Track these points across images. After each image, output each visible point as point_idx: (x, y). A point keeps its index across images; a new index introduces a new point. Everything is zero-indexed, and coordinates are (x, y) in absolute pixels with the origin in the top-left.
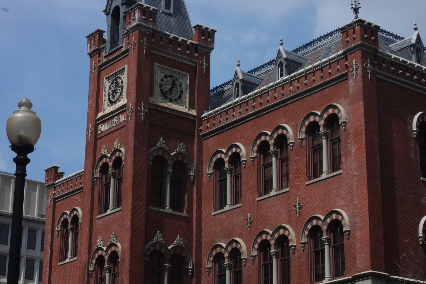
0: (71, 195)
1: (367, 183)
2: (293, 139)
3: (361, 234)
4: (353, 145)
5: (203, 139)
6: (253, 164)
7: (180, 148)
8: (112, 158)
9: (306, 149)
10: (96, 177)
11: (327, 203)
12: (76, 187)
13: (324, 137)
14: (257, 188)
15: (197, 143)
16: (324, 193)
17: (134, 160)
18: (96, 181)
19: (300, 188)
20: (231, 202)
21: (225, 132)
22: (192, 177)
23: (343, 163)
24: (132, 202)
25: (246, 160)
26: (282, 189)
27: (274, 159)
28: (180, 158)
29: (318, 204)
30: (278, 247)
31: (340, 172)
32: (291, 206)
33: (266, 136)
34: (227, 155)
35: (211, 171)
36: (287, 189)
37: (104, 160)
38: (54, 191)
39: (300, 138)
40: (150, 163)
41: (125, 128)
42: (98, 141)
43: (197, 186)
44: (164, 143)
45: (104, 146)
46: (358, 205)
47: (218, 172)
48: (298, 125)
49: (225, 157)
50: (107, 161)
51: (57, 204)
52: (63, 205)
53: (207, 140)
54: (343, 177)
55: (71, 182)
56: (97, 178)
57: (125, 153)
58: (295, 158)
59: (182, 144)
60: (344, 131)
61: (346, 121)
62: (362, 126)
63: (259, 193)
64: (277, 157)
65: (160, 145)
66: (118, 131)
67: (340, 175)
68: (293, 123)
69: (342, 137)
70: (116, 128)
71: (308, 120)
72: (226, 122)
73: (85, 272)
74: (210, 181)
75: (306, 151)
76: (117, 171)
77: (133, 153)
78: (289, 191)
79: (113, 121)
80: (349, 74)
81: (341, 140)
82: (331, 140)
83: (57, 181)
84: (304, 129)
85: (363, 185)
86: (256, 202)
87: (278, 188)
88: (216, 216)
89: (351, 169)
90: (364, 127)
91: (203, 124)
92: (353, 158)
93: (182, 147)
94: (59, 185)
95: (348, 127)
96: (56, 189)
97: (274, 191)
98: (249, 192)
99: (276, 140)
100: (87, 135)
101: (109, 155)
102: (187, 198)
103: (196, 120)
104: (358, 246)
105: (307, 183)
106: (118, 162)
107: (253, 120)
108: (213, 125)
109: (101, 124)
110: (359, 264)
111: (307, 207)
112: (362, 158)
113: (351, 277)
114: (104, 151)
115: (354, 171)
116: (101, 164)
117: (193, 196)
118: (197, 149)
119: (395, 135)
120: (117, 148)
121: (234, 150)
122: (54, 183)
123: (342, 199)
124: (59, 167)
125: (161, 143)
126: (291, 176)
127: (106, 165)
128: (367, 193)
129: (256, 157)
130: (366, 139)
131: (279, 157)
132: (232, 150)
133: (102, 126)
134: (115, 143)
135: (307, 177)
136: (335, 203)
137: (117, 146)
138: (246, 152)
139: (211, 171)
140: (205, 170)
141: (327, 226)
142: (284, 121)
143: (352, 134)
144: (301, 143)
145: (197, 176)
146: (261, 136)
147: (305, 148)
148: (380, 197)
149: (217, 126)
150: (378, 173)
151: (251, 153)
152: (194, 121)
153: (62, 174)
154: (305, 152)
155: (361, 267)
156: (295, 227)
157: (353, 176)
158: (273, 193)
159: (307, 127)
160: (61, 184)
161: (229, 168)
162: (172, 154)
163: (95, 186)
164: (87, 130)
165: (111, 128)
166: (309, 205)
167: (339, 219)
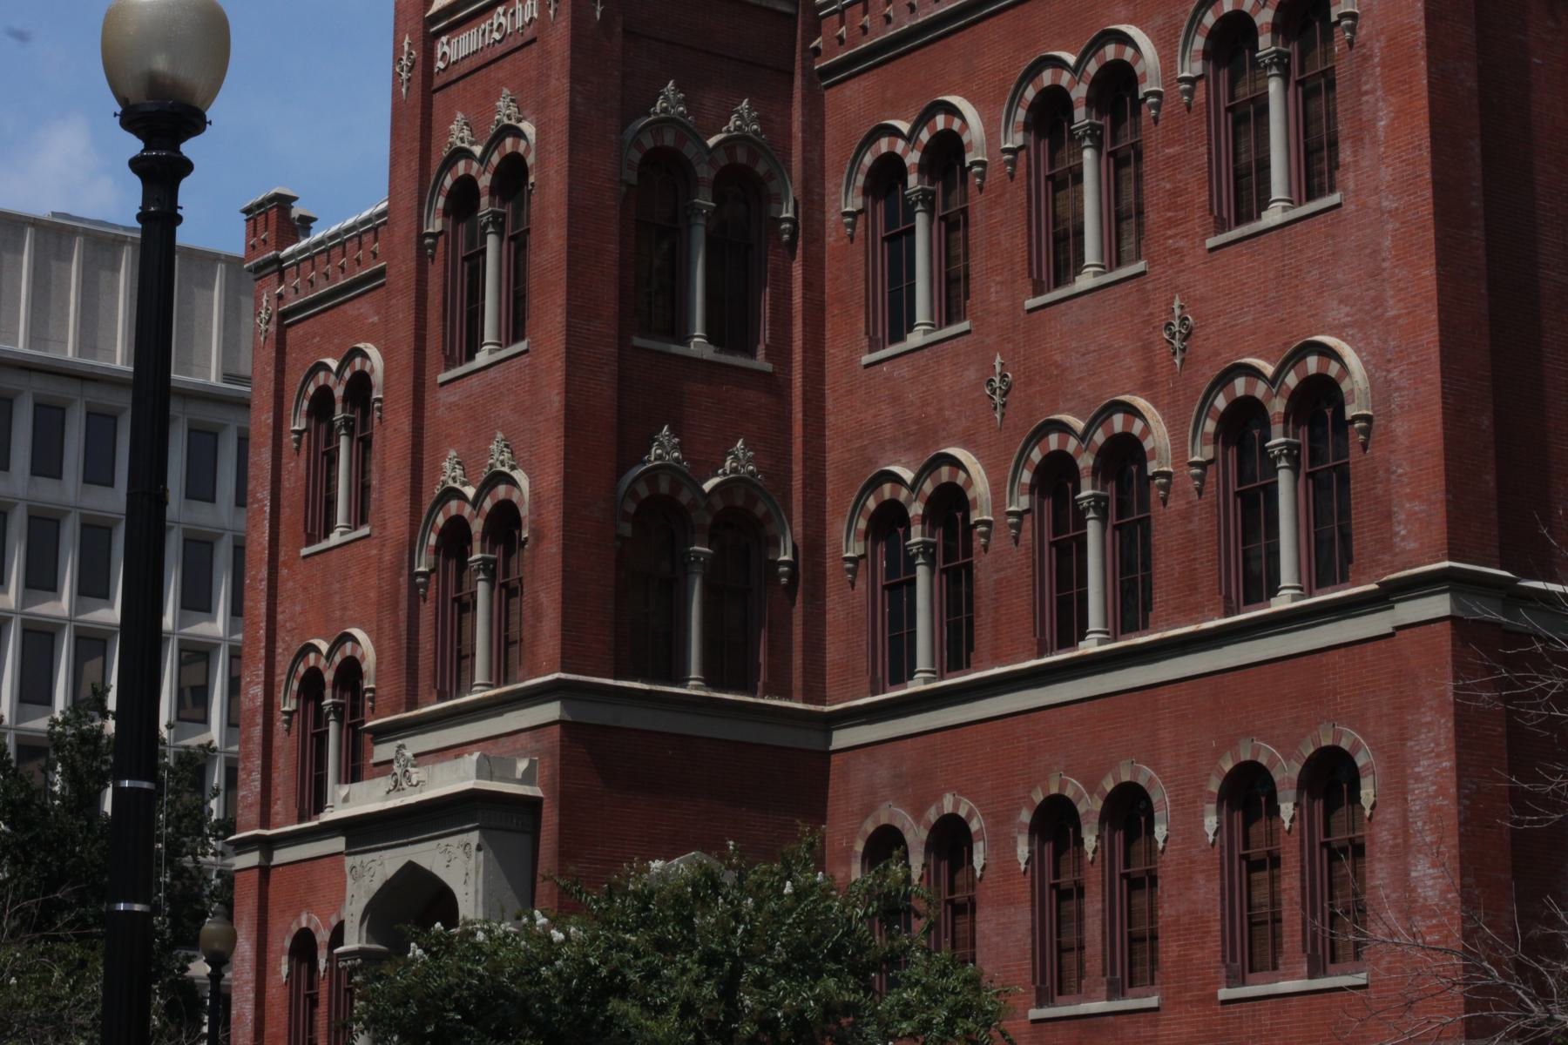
0: (341, 299)
1: (1433, 241)
2: (1158, 79)
3: (1414, 427)
4: (1383, 100)
5: (823, 84)
6: (1012, 176)
7: (741, 117)
8: (489, 160)
9: (1209, 118)
10: (430, 230)
11: (1284, 316)
12: (357, 268)
13: (1274, 71)
14: (1026, 262)
15: (804, 98)
16: (1275, 278)
17: (570, 167)
18: (433, 246)
19: (1188, 260)
20: (932, 317)
21: (907, 58)
22: (788, 225)
23: (1344, 165)
24: (567, 321)
25: (986, 159)
26: (1119, 264)
27: (1088, 154)
28: (741, 157)
29: (1254, 319)
30: (1105, 481)
31: (1335, 198)
32: (1154, 328)
33: (1058, 70)
34: (915, 142)
35: (854, 203)
36: (1140, 266)
37: (461, 167)
38: (279, 285)
39: (1186, 74)
40: (632, 177)
41: (534, 46)
42: (437, 96)
43: (805, 259)
44: (679, 102)
45: (460, 116)
46: (1400, 321)
47: (881, 206)
48: (1177, 28)
49: (905, 151)
50: (473, 173)
51: (291, 334)
52: (314, 337)
53: (839, 87)
54: (1345, 220)
55: (339, 250)
56: (434, 236)
57: (537, 139)
58: (1167, 151)
59: (748, 103)
60: (1348, 49)
61: (1357, 11)
62: (1414, 28)
63: (1033, 280)
64: (1098, 147)
65: (664, 110)
66: (509, 59)
67: (1334, 211)
68: (1159, 20)
69: (1343, 72)
70: (500, 49)
71: (1213, 7)
72: (909, 20)
73: (401, 579)
74: (852, 240)
75: (1209, 125)
76: (508, 209)
77: (565, 138)
78: (1143, 273)
79: (490, 21)
81: (1337, 82)
82: (1299, 83)
83: (289, 250)
84: (1199, 43)
85: (1421, 248)
86: (1022, 314)
87: (1106, 263)
88: (878, 367)
89: (1376, 190)
90: (1422, 33)
91: (824, 29)
92: (1382, 149)
93: (746, 115)
94: (297, 264)
95: (1362, 33)
96: (287, 278)
97: (1091, 274)
98: (998, 279)
99: (1096, 83)
100: (396, 76)
101: (478, 150)
102: (767, 302)
103: (797, 13)
104: (1400, 471)
105: (1211, 242)
106: (512, 175)
107: (1011, 11)
108: (861, 31)
109: (445, 35)
110: (1404, 538)
111: (1213, 332)
112: (1414, 148)
113: (1373, 586)
114: (458, 133)
115: (1387, 198)
116: (448, 182)
117: (790, 294)
118: (804, 123)
119: (1539, 62)
120: (506, 121)
121: (940, 121)
122: (277, 256)
123: (1341, 302)
124: (295, 199)
125: (669, 100)
126: (1152, 216)
127: (466, 186)
128: (1435, 276)
129: (1021, 148)
130: (1429, 77)
131: (1107, 148)
132: (931, 123)
133: (448, 43)
134: (500, 104)
135: (1211, 220)
136: (1317, 315)
137: (509, 117)
138: (985, 132)
139: (854, 203)
140: (833, 197)
141: (1285, 401)
142: (1123, 12)
143: (1377, 60)
144: (1190, 93)
145: (804, 220)
146: (1040, 72)
147: (1205, 114)
148: (1483, 291)
149: (877, 35)
150: (1474, 204)
151: (1002, 135)
152: (792, 18)
153: (306, 222)
154: (1205, 127)
155: (1410, 551)
156: (1168, 404)
157: (1382, 215)
158: (1085, 281)
159: (1212, 35)
160: (303, 260)
161: (922, 190)
162: (712, 142)
163: (430, 264)
164: (394, 58)
165: (485, 49)
166: (1221, 323)
167: (1329, 374)
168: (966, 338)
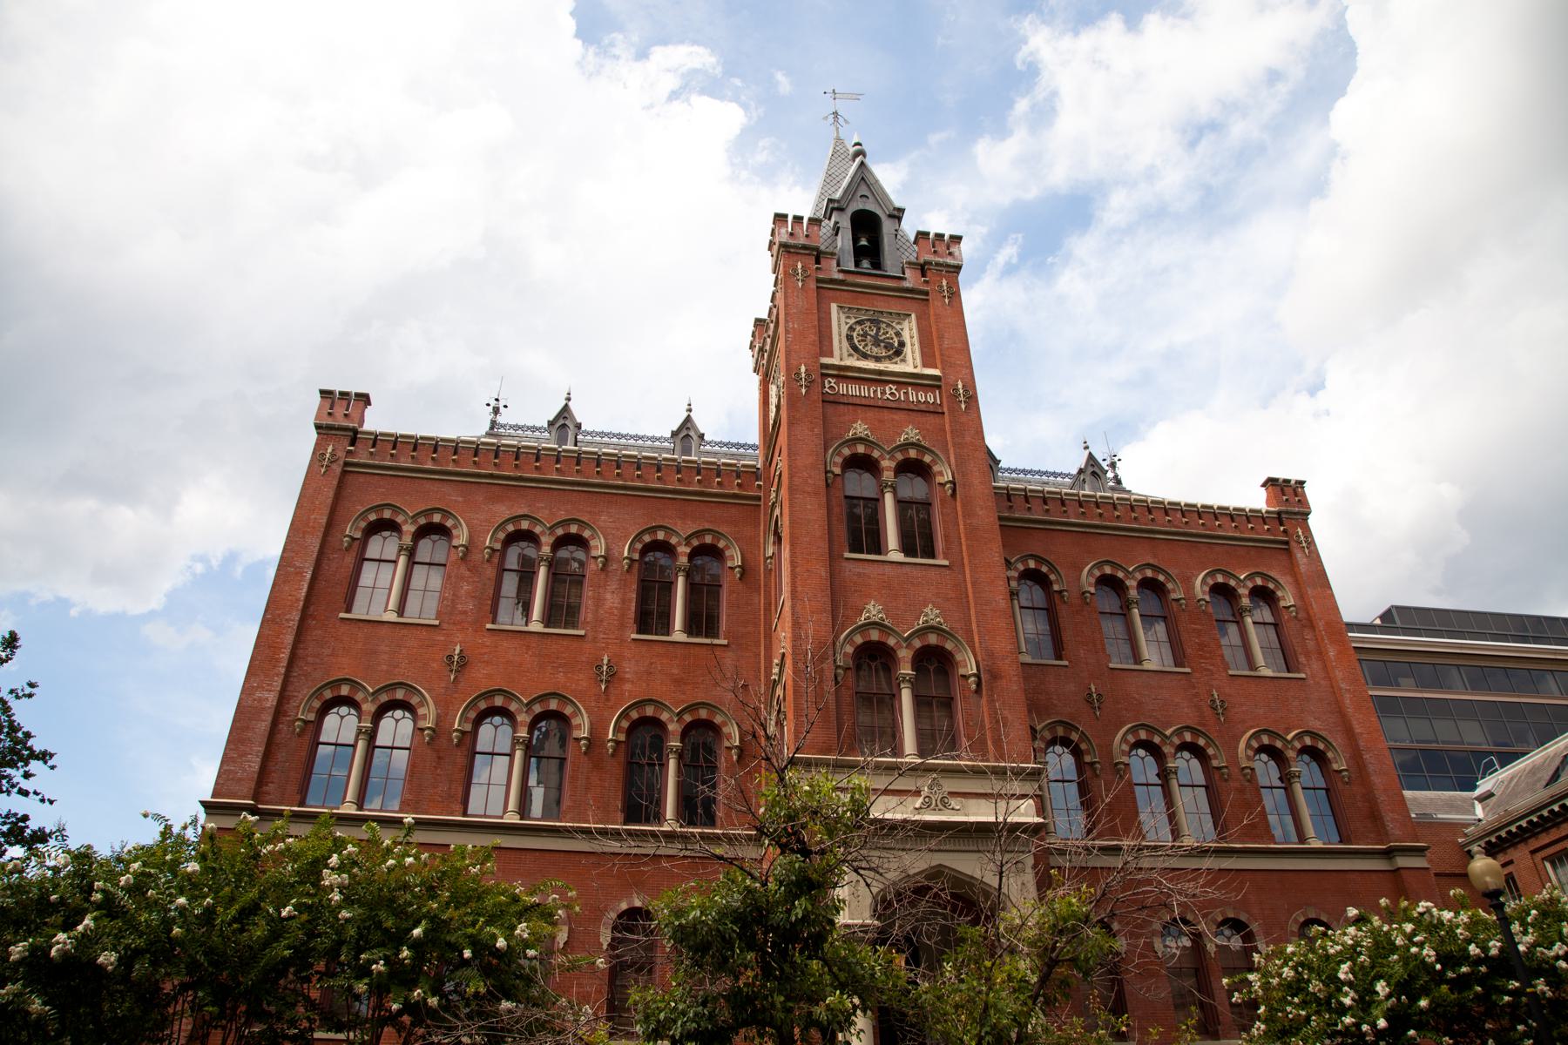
31: (1303, 676)
36: (1187, 670)
73: (825, 666)
80: (1293, 544)
105: (1231, 672)
168: (1065, 669)
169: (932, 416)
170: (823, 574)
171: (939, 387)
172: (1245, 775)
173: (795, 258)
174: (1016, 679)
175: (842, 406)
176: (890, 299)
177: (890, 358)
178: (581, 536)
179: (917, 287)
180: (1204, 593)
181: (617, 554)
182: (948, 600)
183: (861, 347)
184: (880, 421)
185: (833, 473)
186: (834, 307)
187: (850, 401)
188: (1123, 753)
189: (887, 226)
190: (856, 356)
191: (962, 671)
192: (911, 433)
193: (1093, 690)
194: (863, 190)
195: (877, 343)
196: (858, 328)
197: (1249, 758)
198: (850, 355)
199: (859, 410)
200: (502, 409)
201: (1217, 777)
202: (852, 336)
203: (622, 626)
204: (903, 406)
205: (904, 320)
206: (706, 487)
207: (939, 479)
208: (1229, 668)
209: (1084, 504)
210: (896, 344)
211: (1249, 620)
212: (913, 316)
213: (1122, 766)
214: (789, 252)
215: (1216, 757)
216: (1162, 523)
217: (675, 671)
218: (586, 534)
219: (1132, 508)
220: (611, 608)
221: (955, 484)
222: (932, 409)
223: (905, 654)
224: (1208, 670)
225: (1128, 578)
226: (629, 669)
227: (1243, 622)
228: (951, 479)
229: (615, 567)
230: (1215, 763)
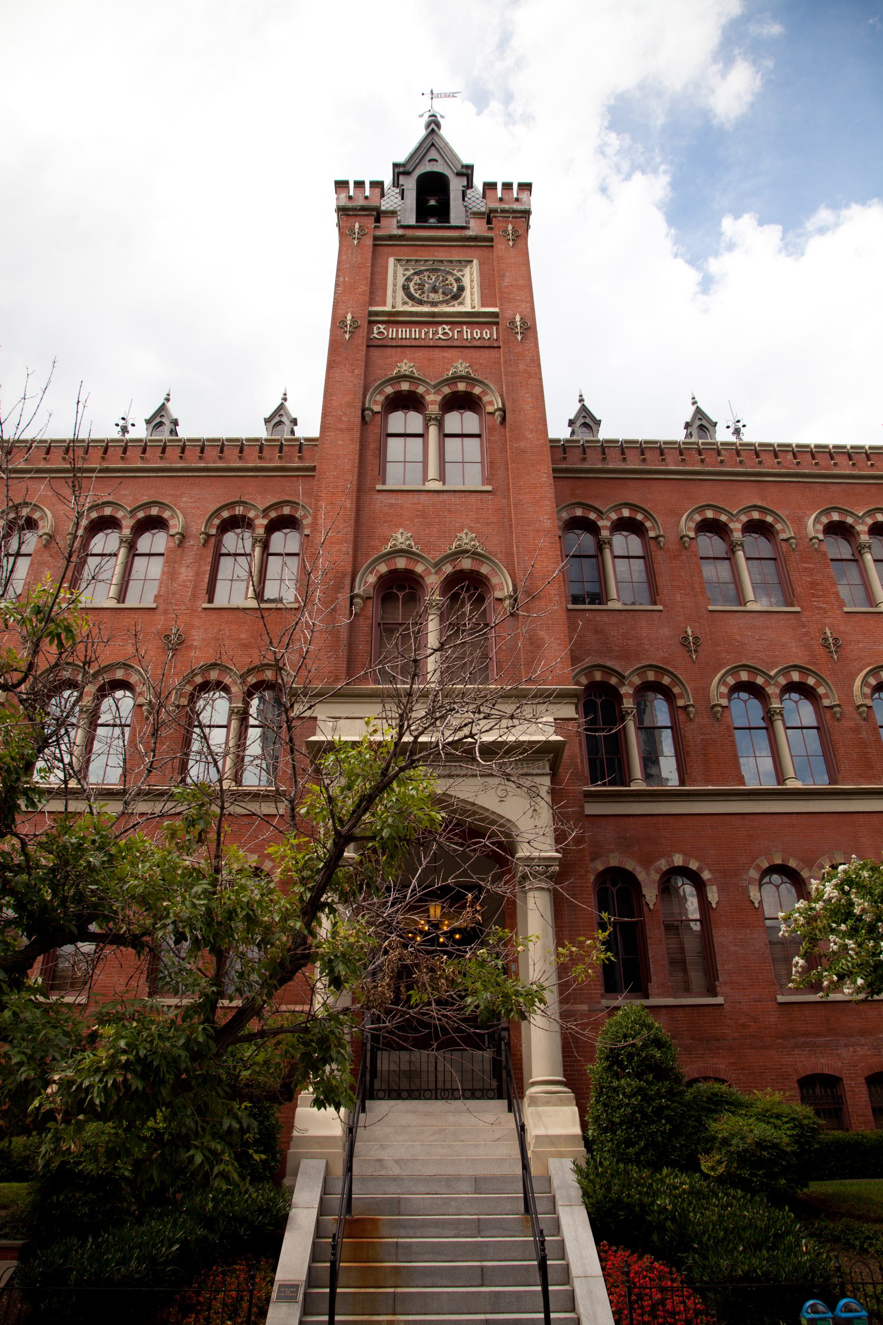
88: (580, 613)
105: (846, 609)
168: (658, 614)
169: (486, 351)
170: (348, 506)
171: (497, 324)
172: (860, 714)
173: (353, 219)
174: (557, 598)
175: (390, 349)
176: (452, 249)
177: (446, 302)
178: (161, 517)
179: (480, 234)
180: (817, 531)
181: (194, 532)
182: (488, 524)
183: (417, 295)
184: (429, 360)
185: (372, 410)
186: (391, 261)
187: (400, 343)
188: (722, 695)
189: (456, 185)
190: (411, 303)
191: (498, 594)
192: (461, 367)
193: (690, 633)
194: (433, 154)
195: (434, 290)
196: (416, 278)
197: (864, 696)
198: (405, 303)
199: (408, 351)
200: (130, 428)
201: (828, 716)
202: (408, 286)
203: (194, 596)
204: (456, 343)
205: (466, 266)
206: (286, 462)
207: (490, 409)
208: (845, 606)
209: (684, 452)
210: (455, 290)
211: (868, 557)
212: (475, 262)
213: (719, 709)
214: (348, 215)
215: (827, 696)
216: (769, 465)
217: (243, 636)
218: (166, 515)
219: (738, 453)
220: (184, 581)
221: (504, 412)
222: (487, 344)
223: (433, 581)
224: (821, 608)
225: (732, 521)
226: (197, 637)
227: (863, 560)
228: (500, 406)
229: (192, 543)
230: (826, 702)
